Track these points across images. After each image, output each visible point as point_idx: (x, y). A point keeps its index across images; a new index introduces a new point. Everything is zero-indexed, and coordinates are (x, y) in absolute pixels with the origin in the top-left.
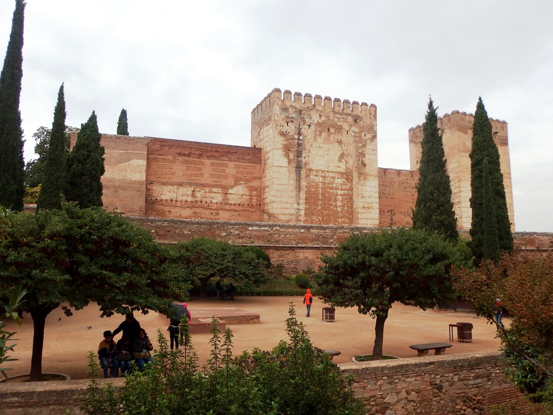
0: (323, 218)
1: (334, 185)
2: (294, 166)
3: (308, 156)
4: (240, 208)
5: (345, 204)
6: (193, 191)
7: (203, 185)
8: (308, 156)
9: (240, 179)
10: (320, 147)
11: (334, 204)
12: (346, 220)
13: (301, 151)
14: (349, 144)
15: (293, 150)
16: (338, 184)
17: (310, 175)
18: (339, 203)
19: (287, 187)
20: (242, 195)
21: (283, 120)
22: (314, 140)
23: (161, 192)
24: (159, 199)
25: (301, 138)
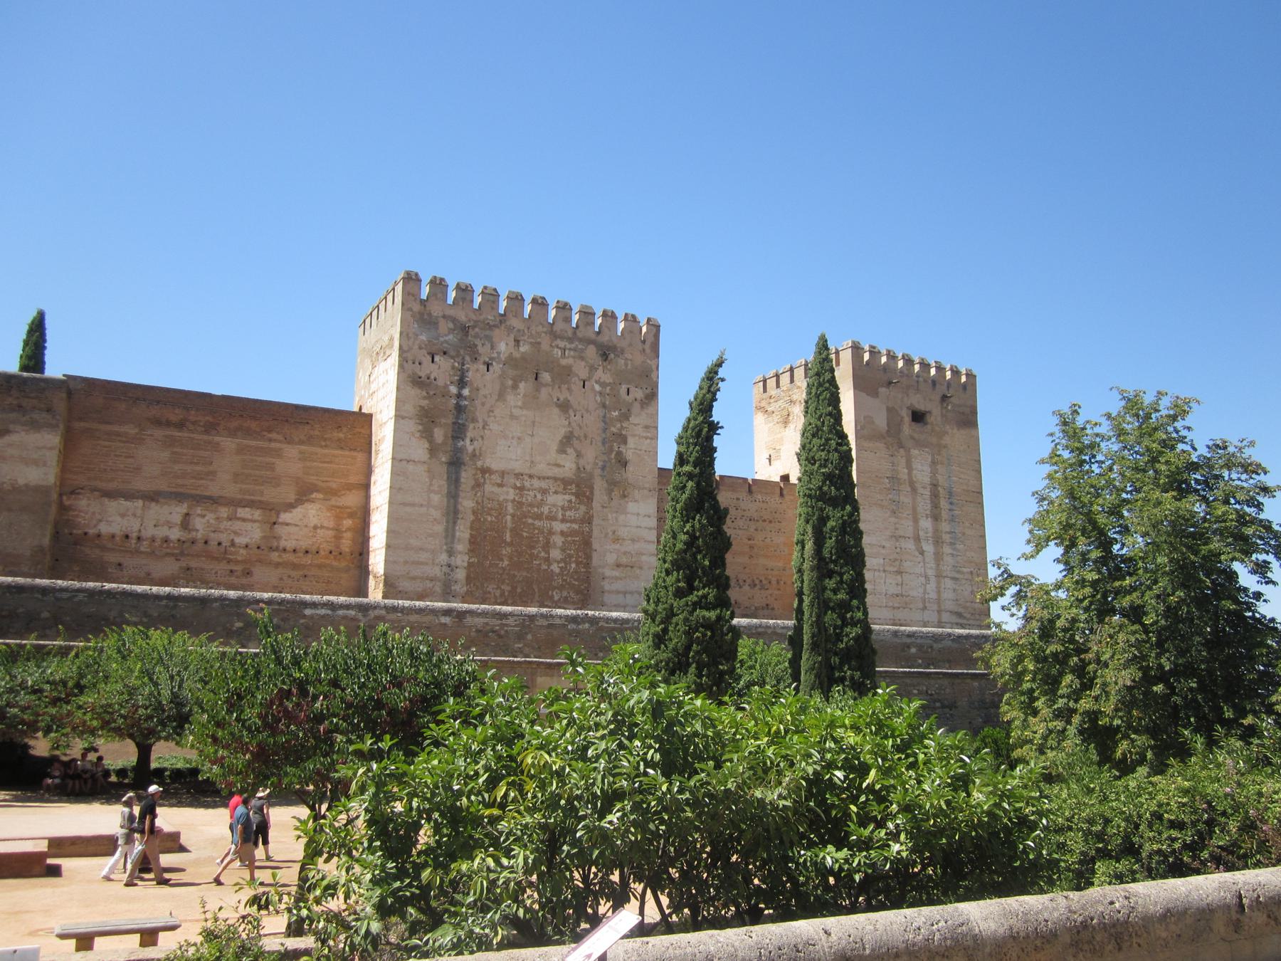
0: (514, 588)
1: (545, 510)
2: (443, 459)
3: (482, 437)
4: (308, 560)
5: (570, 556)
6: (187, 514)
7: (215, 501)
8: (482, 437)
9: (315, 488)
10: (512, 417)
11: (543, 554)
12: (572, 594)
13: (464, 425)
14: (587, 411)
15: (443, 421)
16: (554, 505)
17: (484, 483)
18: (556, 554)
19: (424, 510)
20: (315, 527)
21: (420, 348)
22: (497, 400)
23: (99, 517)
24: (92, 531)
25: (466, 392)
